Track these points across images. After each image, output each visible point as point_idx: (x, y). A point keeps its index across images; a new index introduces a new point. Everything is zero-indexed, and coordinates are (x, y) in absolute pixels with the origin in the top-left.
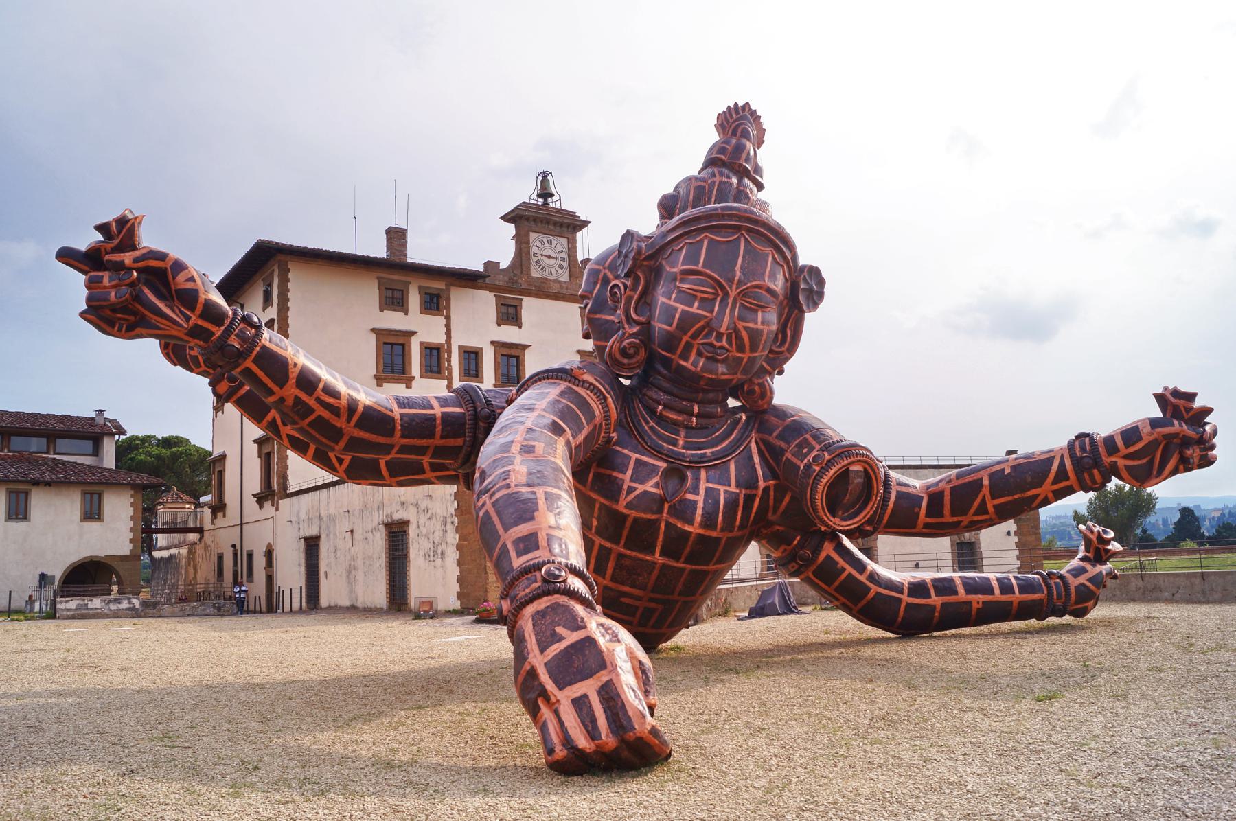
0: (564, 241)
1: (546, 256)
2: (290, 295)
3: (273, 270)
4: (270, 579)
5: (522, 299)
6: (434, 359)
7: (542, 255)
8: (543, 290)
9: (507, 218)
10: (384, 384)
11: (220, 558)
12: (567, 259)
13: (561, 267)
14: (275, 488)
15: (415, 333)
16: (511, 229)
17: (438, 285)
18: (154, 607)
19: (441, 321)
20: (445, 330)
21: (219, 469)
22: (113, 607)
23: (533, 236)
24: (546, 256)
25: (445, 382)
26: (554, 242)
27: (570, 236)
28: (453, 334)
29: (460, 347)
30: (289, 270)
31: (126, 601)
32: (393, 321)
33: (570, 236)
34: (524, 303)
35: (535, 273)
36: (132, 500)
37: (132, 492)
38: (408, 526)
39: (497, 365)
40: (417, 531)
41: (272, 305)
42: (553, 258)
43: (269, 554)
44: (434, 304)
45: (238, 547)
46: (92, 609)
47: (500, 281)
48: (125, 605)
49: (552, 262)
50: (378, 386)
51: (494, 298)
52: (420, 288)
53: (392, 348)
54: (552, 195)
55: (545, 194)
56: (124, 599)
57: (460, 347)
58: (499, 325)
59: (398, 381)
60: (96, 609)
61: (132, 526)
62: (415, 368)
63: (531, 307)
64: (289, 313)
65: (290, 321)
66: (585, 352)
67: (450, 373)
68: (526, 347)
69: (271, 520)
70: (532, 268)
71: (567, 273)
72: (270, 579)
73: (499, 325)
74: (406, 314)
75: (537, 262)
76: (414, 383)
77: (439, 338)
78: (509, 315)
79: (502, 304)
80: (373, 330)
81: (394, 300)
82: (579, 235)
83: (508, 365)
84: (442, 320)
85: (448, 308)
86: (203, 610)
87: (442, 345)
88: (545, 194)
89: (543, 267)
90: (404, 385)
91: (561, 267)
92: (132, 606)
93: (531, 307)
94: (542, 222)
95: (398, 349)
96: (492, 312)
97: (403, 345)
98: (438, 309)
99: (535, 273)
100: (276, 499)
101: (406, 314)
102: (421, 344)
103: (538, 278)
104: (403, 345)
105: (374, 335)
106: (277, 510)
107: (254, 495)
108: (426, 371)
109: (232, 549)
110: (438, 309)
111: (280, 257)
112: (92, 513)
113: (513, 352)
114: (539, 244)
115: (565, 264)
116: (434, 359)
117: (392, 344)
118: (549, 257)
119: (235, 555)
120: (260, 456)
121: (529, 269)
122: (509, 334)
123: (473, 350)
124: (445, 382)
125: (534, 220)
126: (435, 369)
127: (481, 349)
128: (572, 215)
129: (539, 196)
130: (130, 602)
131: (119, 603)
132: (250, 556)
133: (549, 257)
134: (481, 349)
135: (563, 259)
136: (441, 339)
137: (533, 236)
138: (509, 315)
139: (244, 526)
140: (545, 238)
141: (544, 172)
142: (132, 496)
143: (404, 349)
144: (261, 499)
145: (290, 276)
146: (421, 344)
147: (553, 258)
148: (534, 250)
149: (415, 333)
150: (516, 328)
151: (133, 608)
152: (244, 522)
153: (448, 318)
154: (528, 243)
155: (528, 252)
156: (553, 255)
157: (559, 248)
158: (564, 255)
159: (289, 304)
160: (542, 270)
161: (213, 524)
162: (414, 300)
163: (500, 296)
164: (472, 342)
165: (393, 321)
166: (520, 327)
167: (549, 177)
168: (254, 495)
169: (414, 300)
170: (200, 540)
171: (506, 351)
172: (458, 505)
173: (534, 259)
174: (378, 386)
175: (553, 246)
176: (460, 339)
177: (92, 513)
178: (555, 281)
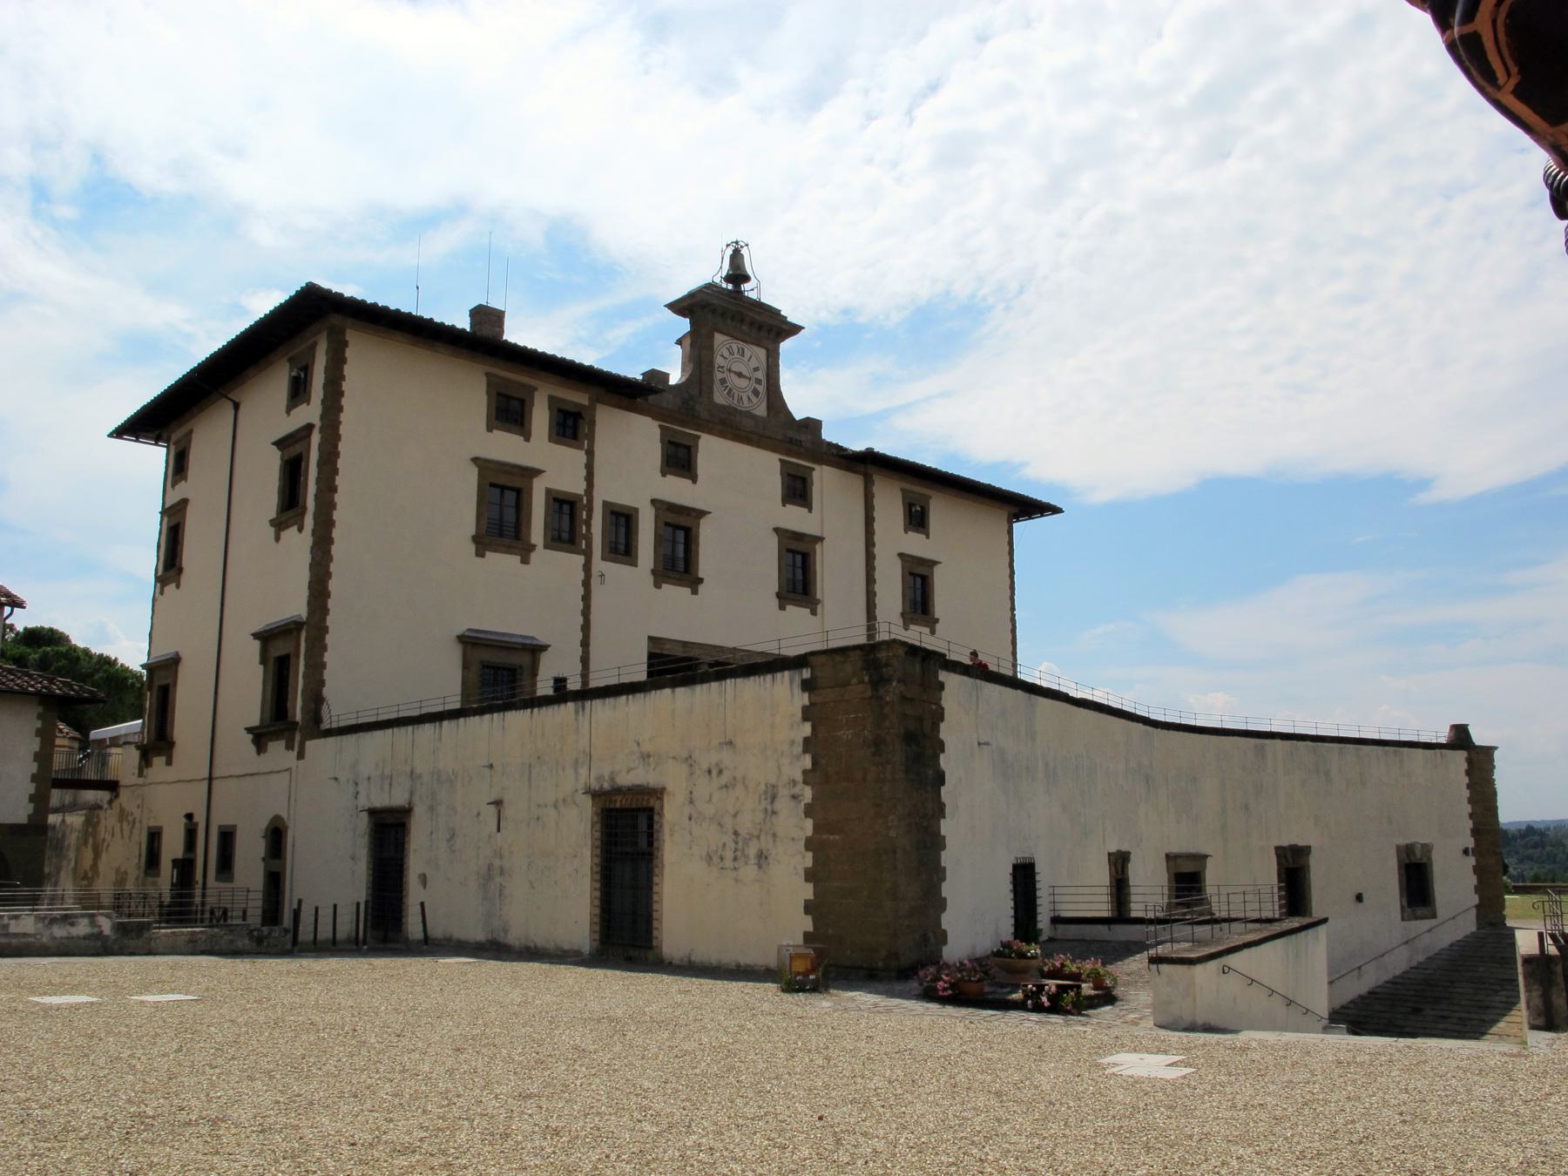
0: (761, 353)
1: (735, 373)
2: (345, 386)
3: (315, 344)
4: (274, 882)
5: (699, 437)
7: (730, 371)
8: (734, 426)
9: (679, 307)
10: (488, 553)
11: (154, 836)
12: (764, 382)
13: (756, 393)
14: (298, 717)
15: (537, 472)
16: (683, 325)
17: (578, 397)
18: (139, 935)
19: (580, 457)
20: (584, 472)
21: (164, 682)
22: (59, 932)
23: (719, 338)
24: (735, 373)
25: (581, 559)
26: (747, 353)
27: (770, 346)
28: (596, 481)
29: (606, 504)
30: (346, 344)
31: (86, 921)
32: (506, 447)
33: (770, 346)
34: (701, 443)
35: (720, 398)
36: (39, 724)
37: (40, 709)
38: (661, 799)
39: (659, 540)
40: (687, 810)
41: (308, 402)
42: (745, 377)
43: (276, 836)
45: (200, 818)
46: (16, 935)
47: (668, 401)
48: (82, 928)
49: (742, 383)
50: (477, 555)
51: (659, 431)
52: (552, 400)
53: (502, 494)
54: (746, 279)
55: (738, 275)
56: (83, 916)
57: (606, 504)
58: (664, 474)
59: (509, 550)
60: (25, 935)
61: (35, 771)
62: (537, 533)
63: (712, 450)
64: (343, 417)
65: (343, 430)
66: (787, 531)
67: (589, 545)
68: (702, 513)
69: (287, 773)
70: (715, 389)
71: (764, 404)
72: (274, 882)
73: (664, 474)
74: (527, 439)
75: (723, 381)
76: (534, 556)
77: (574, 484)
78: (679, 460)
79: (670, 442)
80: (475, 460)
83: (674, 542)
84: (580, 457)
85: (591, 437)
86: (231, 942)
87: (580, 497)
89: (730, 390)
90: (519, 558)
91: (756, 393)
92: (96, 930)
93: (712, 450)
94: (733, 318)
95: (510, 497)
97: (519, 492)
98: (575, 437)
99: (720, 398)
100: (298, 737)
101: (527, 439)
102: (549, 491)
103: (723, 407)
104: (519, 492)
105: (475, 470)
106: (301, 756)
107: (249, 730)
108: (553, 539)
109: (184, 820)
110: (575, 437)
111: (336, 319)
113: (683, 521)
114: (726, 354)
115: (762, 388)
117: (503, 488)
118: (740, 375)
119: (191, 834)
120: (264, 660)
121: (711, 392)
122: (677, 490)
123: (625, 512)
124: (581, 559)
125: (723, 315)
126: (565, 536)
127: (636, 510)
128: (774, 313)
129: (728, 279)
130: (93, 923)
131: (72, 924)
132: (227, 838)
133: (740, 375)
134: (636, 510)
135: (758, 381)
136: (578, 488)
137: (719, 338)
138: (679, 460)
139: (215, 783)
140: (736, 345)
141: (737, 243)
142: (39, 717)
143: (521, 497)
144: (260, 738)
145: (348, 353)
146: (549, 491)
147: (745, 377)
148: (719, 361)
149: (537, 472)
150: (688, 482)
151: (99, 936)
152: (217, 773)
153: (590, 454)
154: (711, 348)
155: (711, 363)
156: (745, 372)
157: (754, 363)
158: (761, 375)
159: (344, 401)
160: (729, 393)
161: (141, 774)
162: (540, 418)
163: (667, 428)
164: (623, 499)
165: (506, 447)
166: (694, 480)
167: (744, 251)
168: (249, 730)
169: (540, 418)
170: (110, 802)
171: (672, 518)
172: (814, 763)
173: (718, 376)
174: (477, 555)
175: (746, 359)
176: (609, 490)
178: (749, 415)
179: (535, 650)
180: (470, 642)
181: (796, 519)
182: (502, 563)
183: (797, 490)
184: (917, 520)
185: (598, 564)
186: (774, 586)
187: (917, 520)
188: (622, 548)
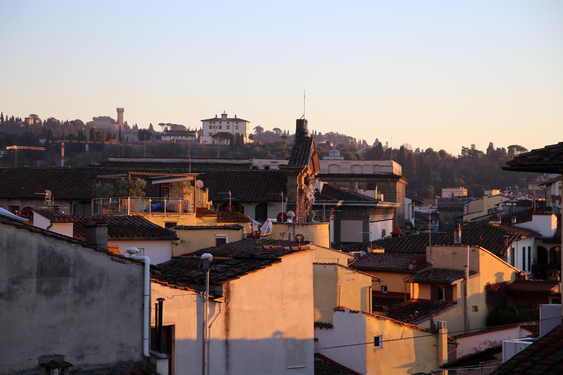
6: (214, 127)
32: (211, 125)
44: (214, 123)
55: (224, 112)
63: (222, 122)
77: (214, 126)
78: (220, 123)
81: (211, 123)
82: (227, 116)
88: (224, 112)
93: (222, 122)
96: (219, 123)
112: (192, 138)
116: (214, 127)
122: (220, 125)
138: (220, 123)
162: (212, 123)
165: (211, 125)
169: (212, 123)
177: (192, 138)
179: (212, 133)
180: (209, 133)
181: (228, 125)
182: (210, 129)
183: (228, 123)
184: (237, 123)
185: (216, 129)
186: (226, 128)
187: (237, 123)
188: (217, 128)
